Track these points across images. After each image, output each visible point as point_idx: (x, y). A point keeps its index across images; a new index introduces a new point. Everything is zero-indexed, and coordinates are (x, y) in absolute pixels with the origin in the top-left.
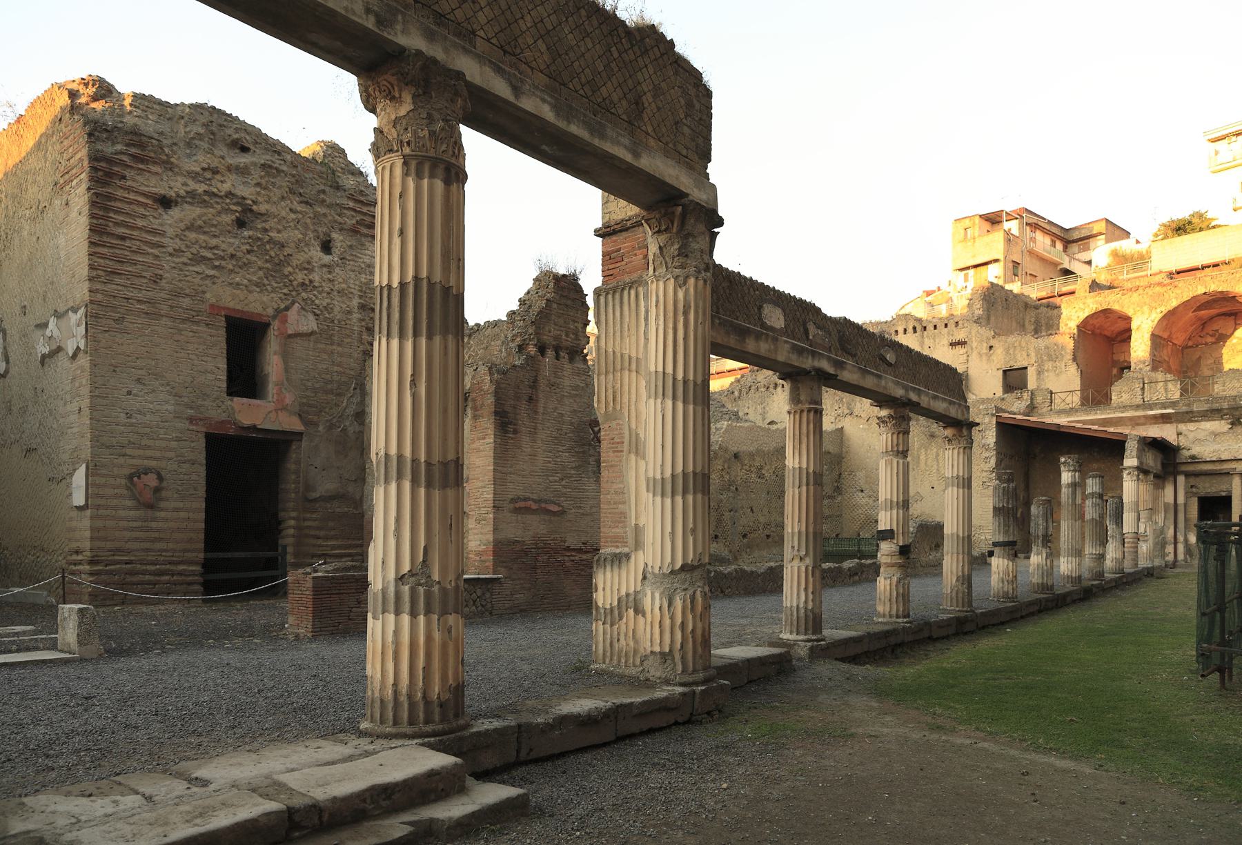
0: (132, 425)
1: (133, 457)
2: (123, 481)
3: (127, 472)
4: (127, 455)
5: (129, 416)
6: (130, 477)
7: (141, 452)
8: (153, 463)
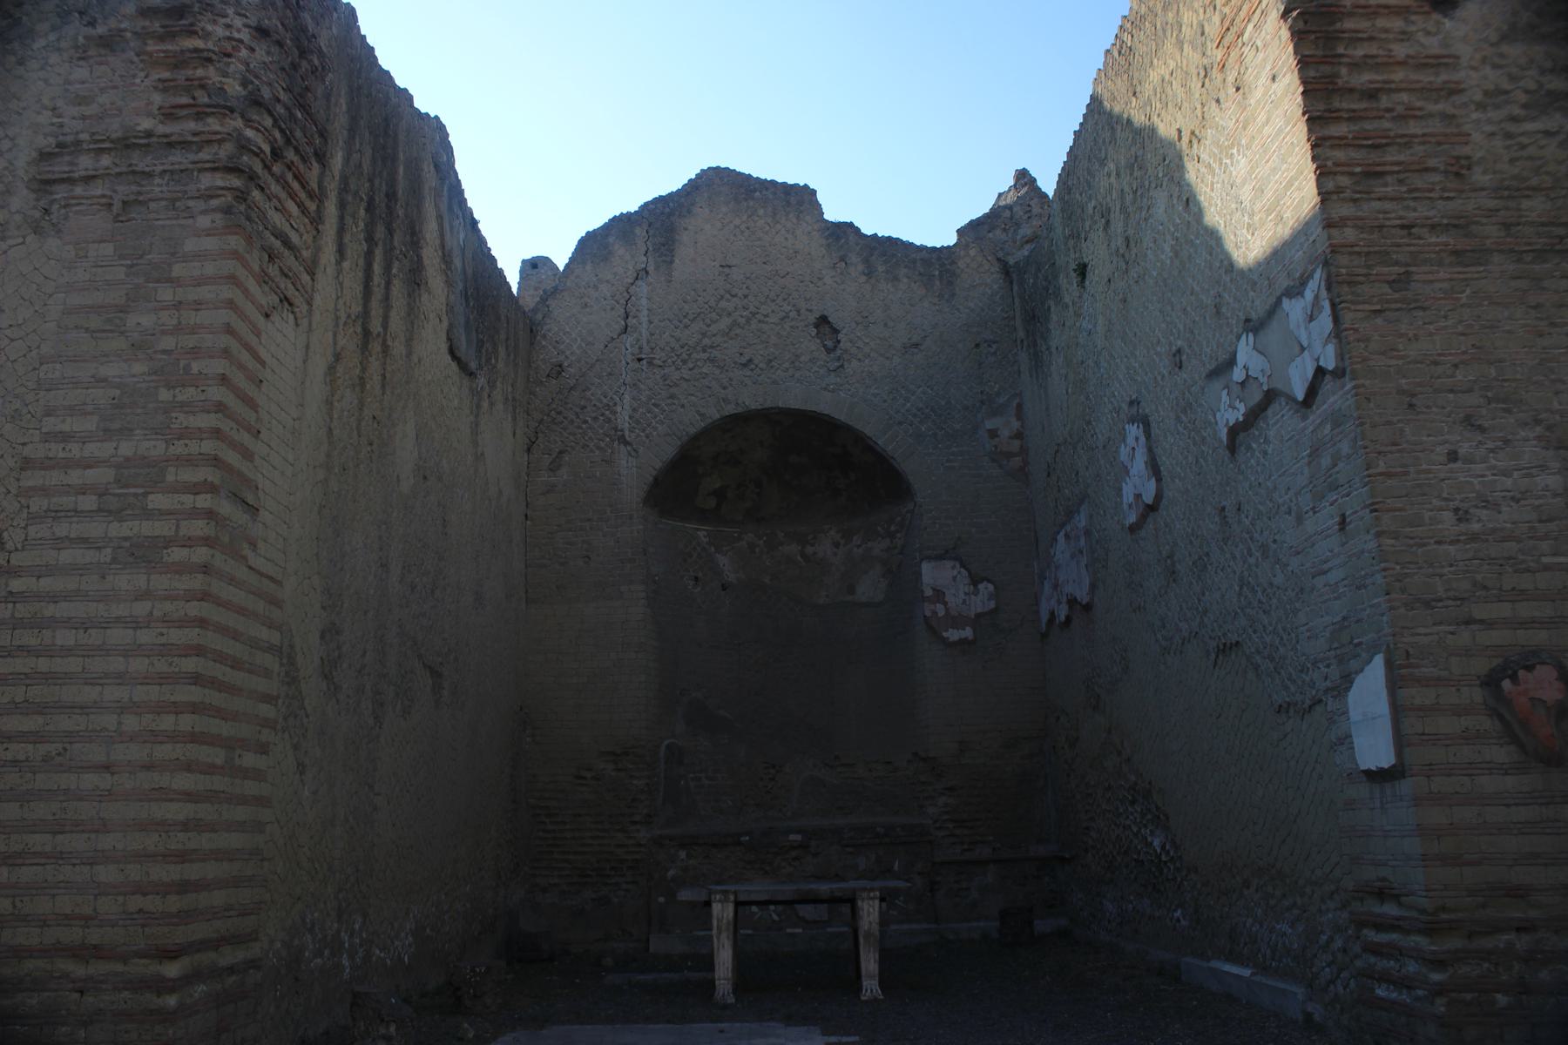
0: (1474, 538)
1: (1488, 624)
2: (1478, 695)
3: (1481, 666)
4: (1475, 622)
5: (1462, 516)
6: (1491, 682)
7: (1505, 610)
8: (1540, 637)
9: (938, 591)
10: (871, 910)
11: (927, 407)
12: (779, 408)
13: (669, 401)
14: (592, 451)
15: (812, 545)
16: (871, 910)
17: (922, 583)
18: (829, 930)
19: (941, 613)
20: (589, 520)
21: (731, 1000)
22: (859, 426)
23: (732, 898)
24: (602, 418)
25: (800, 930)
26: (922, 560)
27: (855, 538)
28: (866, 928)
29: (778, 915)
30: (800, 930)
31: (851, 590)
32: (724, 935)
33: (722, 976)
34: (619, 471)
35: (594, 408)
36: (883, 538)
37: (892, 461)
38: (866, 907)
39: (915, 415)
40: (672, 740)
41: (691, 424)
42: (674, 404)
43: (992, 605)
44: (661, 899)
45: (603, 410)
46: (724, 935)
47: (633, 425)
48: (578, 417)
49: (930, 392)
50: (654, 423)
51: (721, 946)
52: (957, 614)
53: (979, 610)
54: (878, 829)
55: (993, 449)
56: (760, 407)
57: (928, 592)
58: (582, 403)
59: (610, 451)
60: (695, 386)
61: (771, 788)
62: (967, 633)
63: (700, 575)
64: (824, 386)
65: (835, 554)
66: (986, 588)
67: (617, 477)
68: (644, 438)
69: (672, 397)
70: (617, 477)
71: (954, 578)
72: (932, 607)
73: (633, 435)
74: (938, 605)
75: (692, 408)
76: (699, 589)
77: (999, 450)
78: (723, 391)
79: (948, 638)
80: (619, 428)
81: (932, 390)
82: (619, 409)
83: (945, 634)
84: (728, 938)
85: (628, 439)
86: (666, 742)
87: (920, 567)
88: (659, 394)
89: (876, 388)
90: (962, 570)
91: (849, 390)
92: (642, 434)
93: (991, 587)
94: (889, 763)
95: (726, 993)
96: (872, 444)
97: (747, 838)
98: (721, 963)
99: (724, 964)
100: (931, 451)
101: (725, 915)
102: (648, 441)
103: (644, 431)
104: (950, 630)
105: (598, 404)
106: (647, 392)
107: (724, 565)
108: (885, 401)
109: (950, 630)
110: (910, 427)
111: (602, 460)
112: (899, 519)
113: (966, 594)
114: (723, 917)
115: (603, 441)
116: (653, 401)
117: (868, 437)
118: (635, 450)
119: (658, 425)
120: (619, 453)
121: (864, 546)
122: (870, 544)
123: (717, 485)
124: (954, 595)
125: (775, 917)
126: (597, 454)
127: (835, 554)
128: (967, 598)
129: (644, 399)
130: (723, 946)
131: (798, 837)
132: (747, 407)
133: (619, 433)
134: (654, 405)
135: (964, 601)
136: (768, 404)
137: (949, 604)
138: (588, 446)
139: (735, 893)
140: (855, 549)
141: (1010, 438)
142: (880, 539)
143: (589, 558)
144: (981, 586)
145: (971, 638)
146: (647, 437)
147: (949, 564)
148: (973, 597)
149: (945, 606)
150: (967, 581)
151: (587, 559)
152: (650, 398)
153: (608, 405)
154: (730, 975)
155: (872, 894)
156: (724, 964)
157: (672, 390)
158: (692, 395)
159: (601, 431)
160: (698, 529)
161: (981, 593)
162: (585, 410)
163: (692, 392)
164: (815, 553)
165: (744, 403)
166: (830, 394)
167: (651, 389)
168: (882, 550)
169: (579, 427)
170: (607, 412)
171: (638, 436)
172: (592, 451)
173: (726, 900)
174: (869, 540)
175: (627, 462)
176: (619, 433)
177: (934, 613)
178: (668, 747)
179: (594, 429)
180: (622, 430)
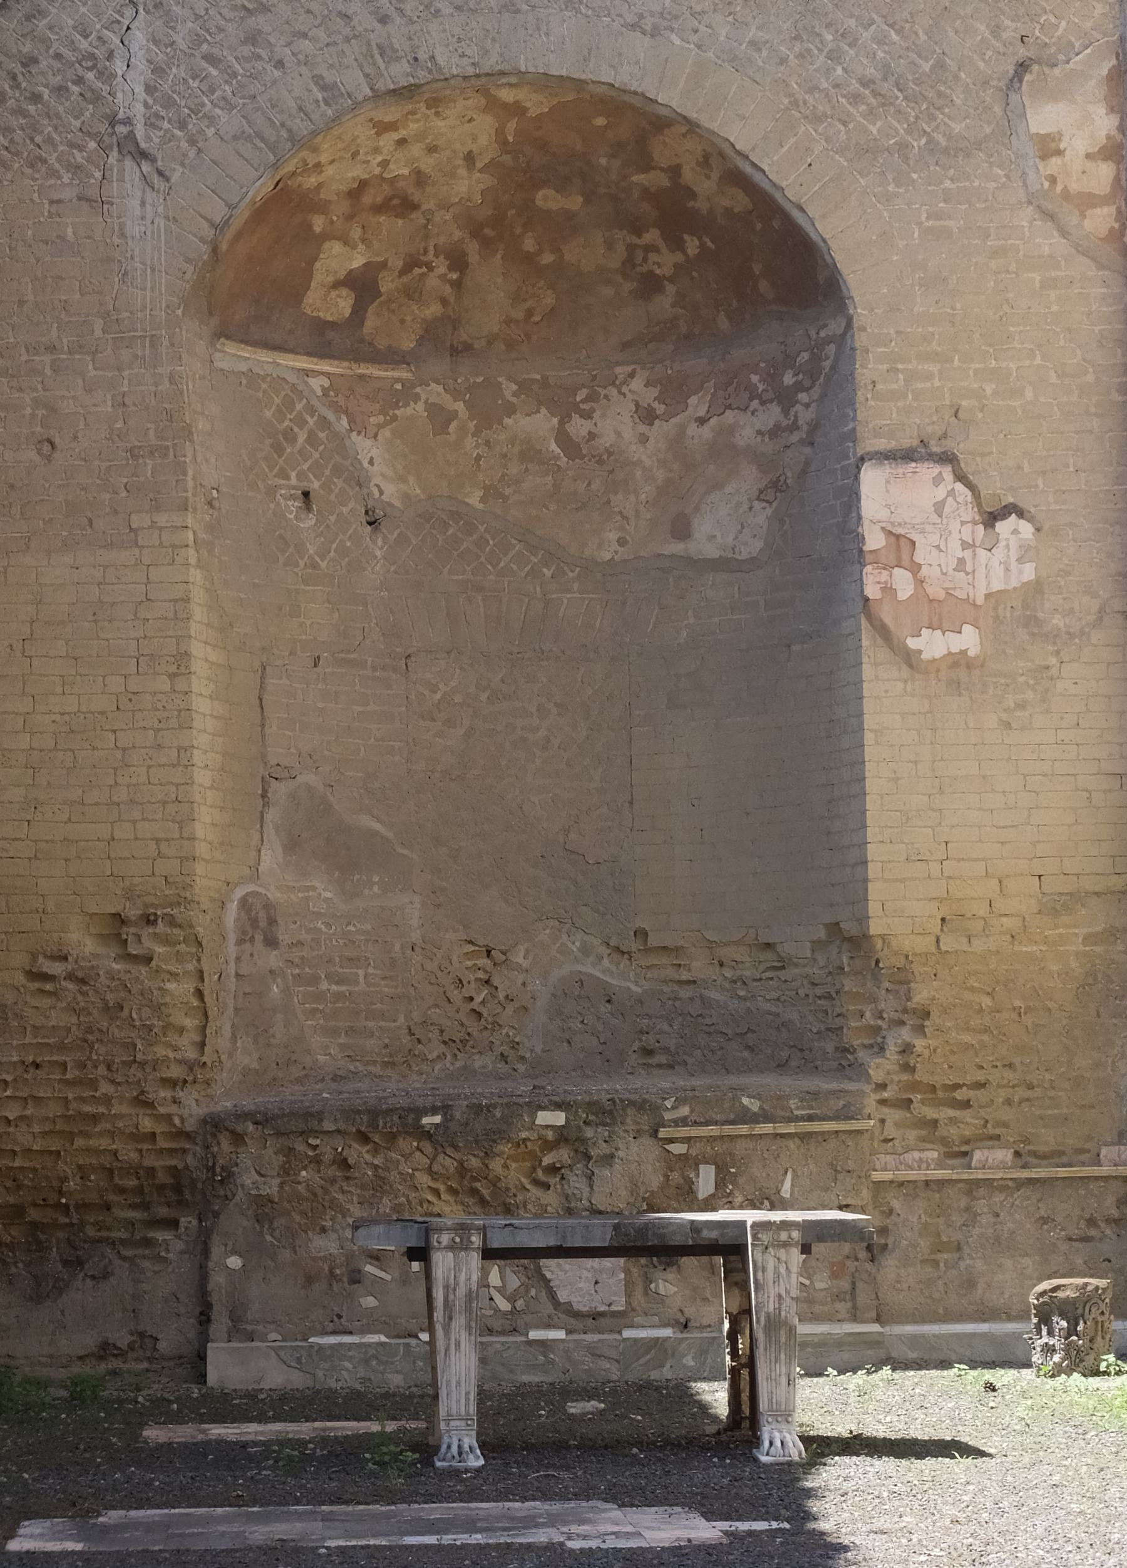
9: (898, 537)
10: (783, 1271)
11: (885, 79)
12: (519, 72)
13: (246, 51)
14: (53, 174)
15: (587, 415)
16: (783, 1271)
17: (860, 518)
18: (628, 1333)
19: (903, 583)
20: (51, 348)
21: (476, 1461)
22: (712, 122)
23: (476, 1240)
24: (75, 89)
25: (561, 1334)
26: (862, 459)
27: (693, 400)
28: (771, 1308)
29: (512, 1299)
30: (561, 1334)
31: (681, 529)
32: (459, 1322)
33: (454, 1411)
34: (122, 226)
35: (57, 64)
36: (763, 403)
37: (795, 214)
38: (771, 1264)
39: (855, 99)
40: (251, 888)
41: (301, 109)
42: (259, 57)
43: (1029, 572)
44: (234, 1262)
45: (80, 71)
46: (459, 1322)
47: (157, 108)
48: (17, 86)
49: (895, 37)
50: (209, 105)
51: (453, 1347)
52: (941, 595)
53: (996, 586)
54: (745, 1101)
55: (1046, 184)
56: (470, 71)
57: (874, 540)
58: (25, 50)
59: (98, 175)
60: (309, 12)
61: (483, 1002)
62: (968, 640)
63: (315, 485)
64: (630, 18)
65: (644, 439)
66: (1015, 532)
67: (116, 241)
68: (184, 144)
69: (253, 39)
70: (116, 241)
71: (939, 508)
72: (884, 576)
73: (156, 135)
74: (896, 570)
75: (304, 70)
76: (311, 521)
77: (1059, 188)
78: (378, 26)
79: (920, 652)
80: (121, 115)
81: (900, 32)
82: (119, 66)
83: (912, 643)
84: (469, 1328)
85: (143, 145)
86: (239, 893)
87: (857, 478)
88: (220, 30)
89: (760, 28)
90: (959, 487)
91: (696, 31)
92: (179, 133)
93: (1026, 529)
94: (768, 945)
95: (466, 1447)
96: (748, 169)
97: (437, 1119)
98: (454, 1384)
99: (458, 1383)
100: (891, 188)
101: (462, 1277)
102: (192, 153)
103: (182, 125)
104: (924, 631)
105: (66, 52)
106: (190, 25)
107: (371, 462)
108: (783, 61)
109: (924, 631)
110: (842, 128)
111: (79, 199)
112: (805, 356)
113: (965, 545)
114: (456, 1284)
115: (81, 148)
116: (205, 46)
117: (739, 153)
118: (160, 173)
119: (218, 111)
120: (121, 180)
121: (714, 421)
122: (730, 416)
123: (357, 262)
124: (938, 547)
125: (503, 1305)
126: (66, 180)
127: (644, 439)
128: (968, 554)
129: (182, 44)
130: (458, 1345)
131: (558, 1118)
132: (440, 69)
133: (121, 129)
134: (210, 58)
135: (961, 561)
136: (491, 63)
137: (925, 571)
138: (44, 161)
139: (484, 1230)
140: (692, 429)
141: (1088, 156)
142: (755, 403)
143: (53, 445)
144: (1003, 527)
145: (971, 653)
146: (192, 142)
147: (927, 471)
148: (982, 553)
149: (915, 575)
150: (970, 513)
151: (46, 447)
152: (198, 41)
153: (92, 57)
154: (473, 1409)
155: (784, 1236)
156: (458, 1383)
157: (251, 21)
158: (304, 35)
159: (77, 123)
160: (307, 373)
161: (1002, 544)
162: (34, 69)
163: (303, 28)
164: (592, 436)
165: (432, 58)
166: (647, 40)
167: (198, 17)
168: (759, 433)
169: (21, 112)
170: (90, 75)
171: (170, 138)
172: (54, 174)
173: (465, 1247)
174: (729, 407)
175: (143, 203)
176: (121, 129)
177: (889, 590)
178: (244, 903)
179: (58, 115)
180: (128, 121)
